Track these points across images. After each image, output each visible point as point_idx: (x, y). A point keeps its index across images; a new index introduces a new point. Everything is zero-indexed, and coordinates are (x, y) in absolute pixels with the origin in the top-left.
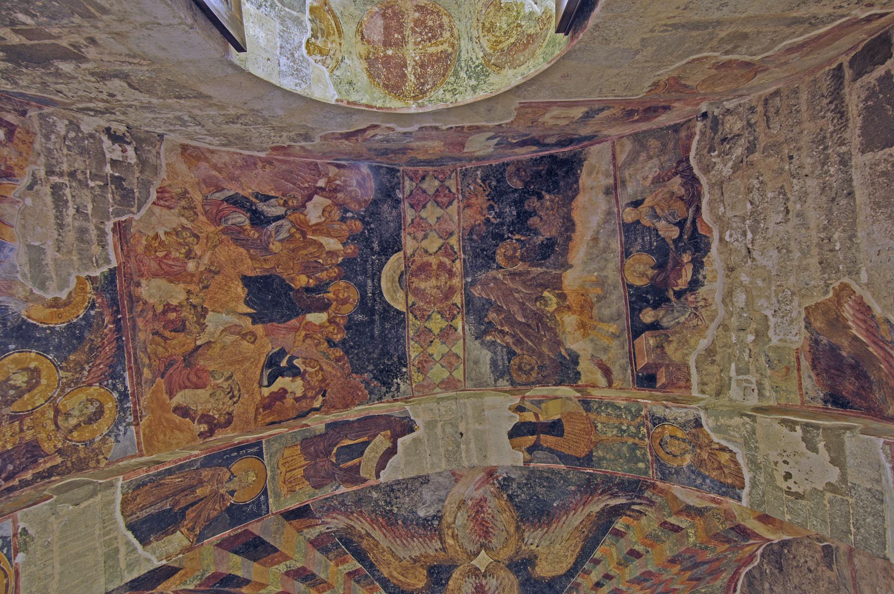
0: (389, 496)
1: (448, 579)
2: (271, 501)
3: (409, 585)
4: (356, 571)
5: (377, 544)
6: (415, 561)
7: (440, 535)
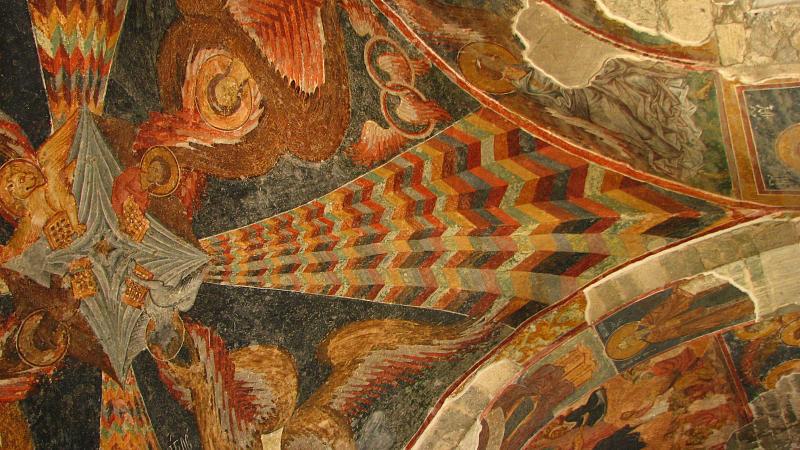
0: (423, 396)
1: (299, 382)
2: (596, 336)
3: (349, 333)
4: (425, 298)
5: (411, 341)
6: (355, 363)
7: (341, 417)
